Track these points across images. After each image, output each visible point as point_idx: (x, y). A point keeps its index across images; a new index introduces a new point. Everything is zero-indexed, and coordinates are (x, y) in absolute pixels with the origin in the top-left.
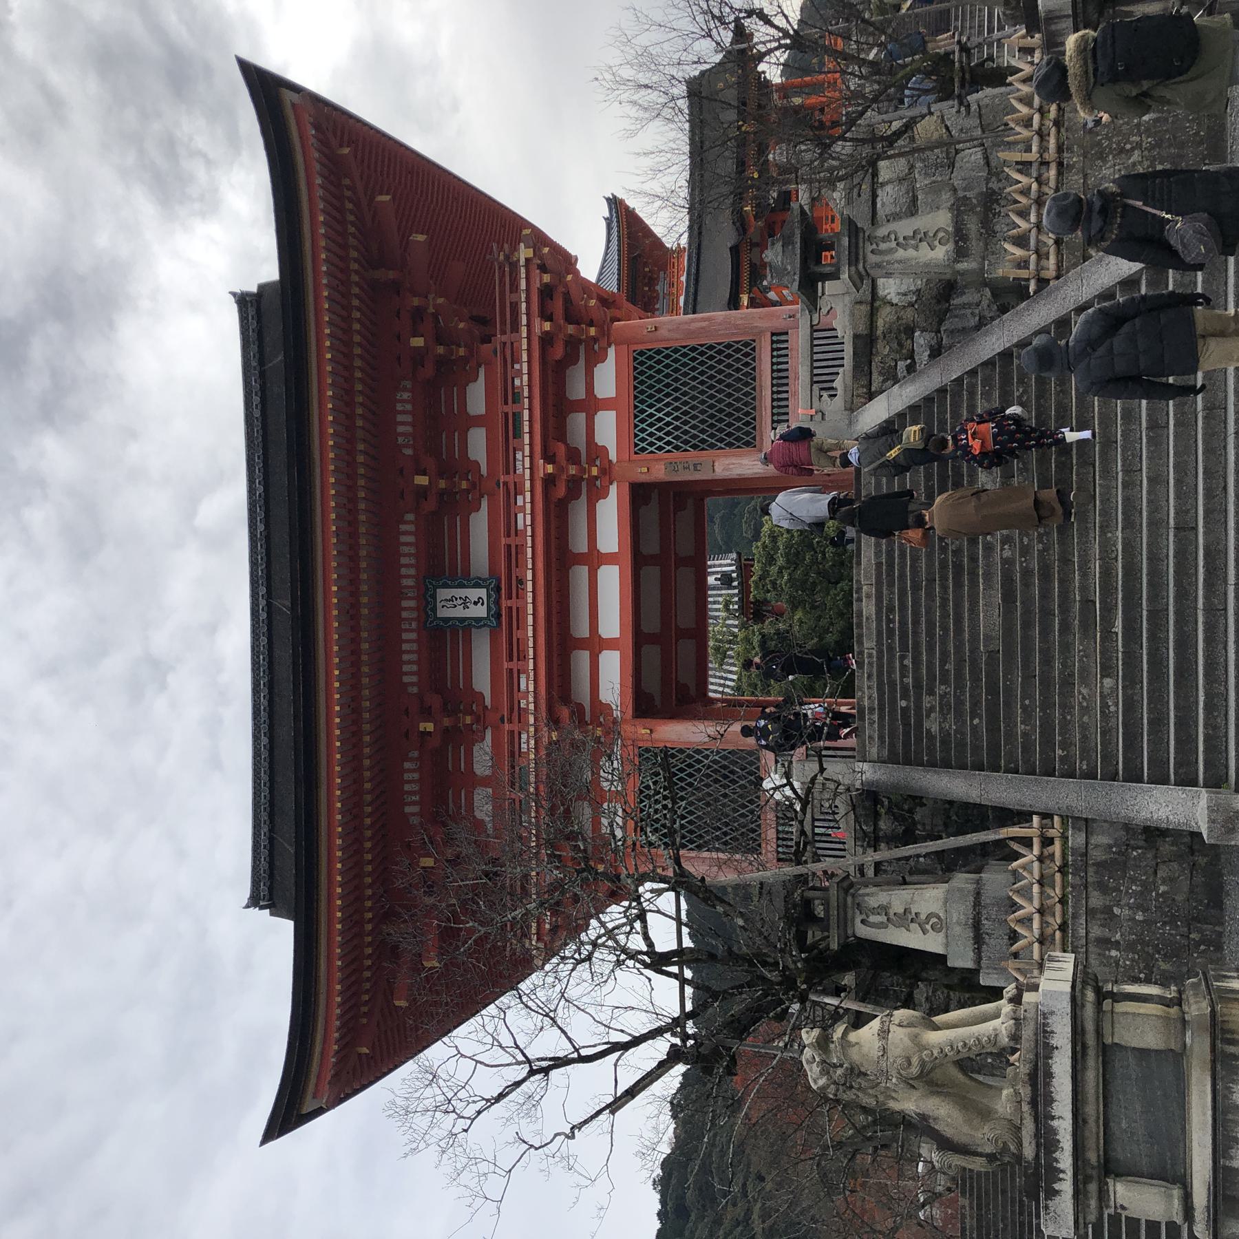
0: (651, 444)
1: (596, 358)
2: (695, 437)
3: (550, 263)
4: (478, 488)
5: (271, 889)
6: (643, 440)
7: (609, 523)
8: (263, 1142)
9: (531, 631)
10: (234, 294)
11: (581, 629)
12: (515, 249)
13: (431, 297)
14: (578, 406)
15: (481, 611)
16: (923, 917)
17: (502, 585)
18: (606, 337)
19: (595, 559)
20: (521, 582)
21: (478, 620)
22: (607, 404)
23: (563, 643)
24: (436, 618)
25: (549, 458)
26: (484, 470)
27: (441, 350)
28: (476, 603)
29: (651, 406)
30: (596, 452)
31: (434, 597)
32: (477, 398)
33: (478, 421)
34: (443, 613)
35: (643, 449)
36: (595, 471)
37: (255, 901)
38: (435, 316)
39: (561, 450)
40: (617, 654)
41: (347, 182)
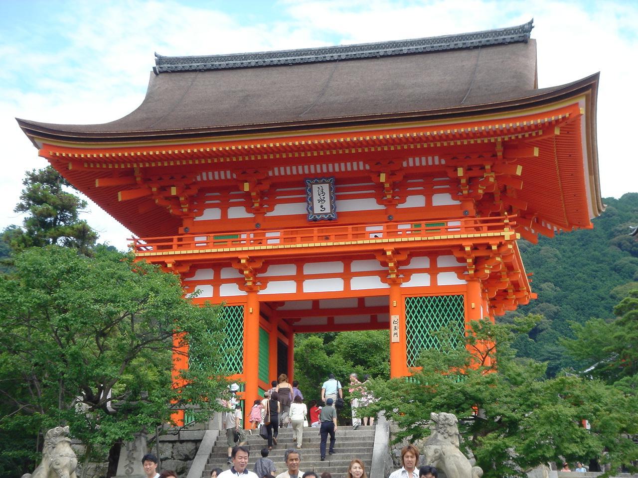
0: (411, 307)
1: (460, 272)
2: (414, 332)
3: (503, 250)
4: (390, 203)
5: (166, 72)
6: (413, 302)
7: (367, 284)
8: (22, 123)
9: (300, 246)
10: (532, 22)
11: (308, 269)
12: (513, 227)
13: (493, 174)
14: (433, 262)
15: (317, 210)
16: (132, 466)
17: (332, 222)
18: (471, 279)
19: (347, 276)
20: (327, 238)
21: (312, 208)
22: (434, 280)
23: (300, 260)
24: (312, 184)
25: (396, 252)
26: (400, 206)
27: (463, 181)
28: (322, 206)
29: (432, 306)
30: (407, 275)
31: (324, 182)
32: (442, 200)
33: (429, 201)
34: (315, 188)
35: (408, 302)
36: (393, 276)
37: (160, 60)
38: (483, 177)
39: (403, 257)
40: (295, 291)
41: (541, 133)
